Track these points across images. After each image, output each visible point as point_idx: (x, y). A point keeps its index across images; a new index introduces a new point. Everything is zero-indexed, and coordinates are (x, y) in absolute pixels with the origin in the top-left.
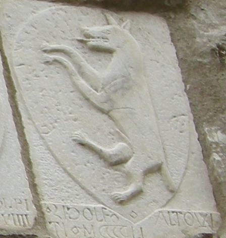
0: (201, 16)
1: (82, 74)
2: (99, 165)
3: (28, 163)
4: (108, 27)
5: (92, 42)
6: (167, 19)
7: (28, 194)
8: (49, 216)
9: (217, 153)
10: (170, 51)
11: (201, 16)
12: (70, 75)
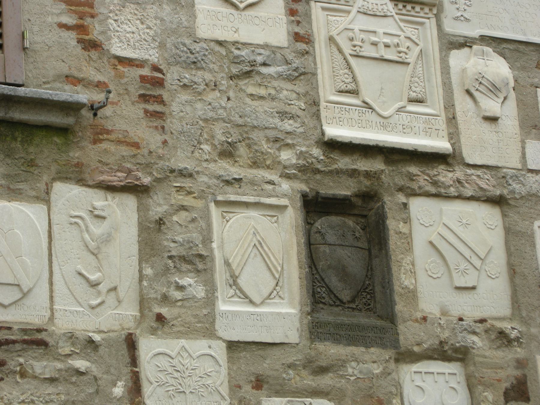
0: (155, 197)
1: (88, 231)
2: (85, 285)
3: (51, 283)
4: (106, 203)
5: (96, 212)
6: (138, 197)
7: (47, 304)
8: (57, 315)
9: (146, 281)
10: (134, 217)
11: (155, 197)
12: (82, 232)
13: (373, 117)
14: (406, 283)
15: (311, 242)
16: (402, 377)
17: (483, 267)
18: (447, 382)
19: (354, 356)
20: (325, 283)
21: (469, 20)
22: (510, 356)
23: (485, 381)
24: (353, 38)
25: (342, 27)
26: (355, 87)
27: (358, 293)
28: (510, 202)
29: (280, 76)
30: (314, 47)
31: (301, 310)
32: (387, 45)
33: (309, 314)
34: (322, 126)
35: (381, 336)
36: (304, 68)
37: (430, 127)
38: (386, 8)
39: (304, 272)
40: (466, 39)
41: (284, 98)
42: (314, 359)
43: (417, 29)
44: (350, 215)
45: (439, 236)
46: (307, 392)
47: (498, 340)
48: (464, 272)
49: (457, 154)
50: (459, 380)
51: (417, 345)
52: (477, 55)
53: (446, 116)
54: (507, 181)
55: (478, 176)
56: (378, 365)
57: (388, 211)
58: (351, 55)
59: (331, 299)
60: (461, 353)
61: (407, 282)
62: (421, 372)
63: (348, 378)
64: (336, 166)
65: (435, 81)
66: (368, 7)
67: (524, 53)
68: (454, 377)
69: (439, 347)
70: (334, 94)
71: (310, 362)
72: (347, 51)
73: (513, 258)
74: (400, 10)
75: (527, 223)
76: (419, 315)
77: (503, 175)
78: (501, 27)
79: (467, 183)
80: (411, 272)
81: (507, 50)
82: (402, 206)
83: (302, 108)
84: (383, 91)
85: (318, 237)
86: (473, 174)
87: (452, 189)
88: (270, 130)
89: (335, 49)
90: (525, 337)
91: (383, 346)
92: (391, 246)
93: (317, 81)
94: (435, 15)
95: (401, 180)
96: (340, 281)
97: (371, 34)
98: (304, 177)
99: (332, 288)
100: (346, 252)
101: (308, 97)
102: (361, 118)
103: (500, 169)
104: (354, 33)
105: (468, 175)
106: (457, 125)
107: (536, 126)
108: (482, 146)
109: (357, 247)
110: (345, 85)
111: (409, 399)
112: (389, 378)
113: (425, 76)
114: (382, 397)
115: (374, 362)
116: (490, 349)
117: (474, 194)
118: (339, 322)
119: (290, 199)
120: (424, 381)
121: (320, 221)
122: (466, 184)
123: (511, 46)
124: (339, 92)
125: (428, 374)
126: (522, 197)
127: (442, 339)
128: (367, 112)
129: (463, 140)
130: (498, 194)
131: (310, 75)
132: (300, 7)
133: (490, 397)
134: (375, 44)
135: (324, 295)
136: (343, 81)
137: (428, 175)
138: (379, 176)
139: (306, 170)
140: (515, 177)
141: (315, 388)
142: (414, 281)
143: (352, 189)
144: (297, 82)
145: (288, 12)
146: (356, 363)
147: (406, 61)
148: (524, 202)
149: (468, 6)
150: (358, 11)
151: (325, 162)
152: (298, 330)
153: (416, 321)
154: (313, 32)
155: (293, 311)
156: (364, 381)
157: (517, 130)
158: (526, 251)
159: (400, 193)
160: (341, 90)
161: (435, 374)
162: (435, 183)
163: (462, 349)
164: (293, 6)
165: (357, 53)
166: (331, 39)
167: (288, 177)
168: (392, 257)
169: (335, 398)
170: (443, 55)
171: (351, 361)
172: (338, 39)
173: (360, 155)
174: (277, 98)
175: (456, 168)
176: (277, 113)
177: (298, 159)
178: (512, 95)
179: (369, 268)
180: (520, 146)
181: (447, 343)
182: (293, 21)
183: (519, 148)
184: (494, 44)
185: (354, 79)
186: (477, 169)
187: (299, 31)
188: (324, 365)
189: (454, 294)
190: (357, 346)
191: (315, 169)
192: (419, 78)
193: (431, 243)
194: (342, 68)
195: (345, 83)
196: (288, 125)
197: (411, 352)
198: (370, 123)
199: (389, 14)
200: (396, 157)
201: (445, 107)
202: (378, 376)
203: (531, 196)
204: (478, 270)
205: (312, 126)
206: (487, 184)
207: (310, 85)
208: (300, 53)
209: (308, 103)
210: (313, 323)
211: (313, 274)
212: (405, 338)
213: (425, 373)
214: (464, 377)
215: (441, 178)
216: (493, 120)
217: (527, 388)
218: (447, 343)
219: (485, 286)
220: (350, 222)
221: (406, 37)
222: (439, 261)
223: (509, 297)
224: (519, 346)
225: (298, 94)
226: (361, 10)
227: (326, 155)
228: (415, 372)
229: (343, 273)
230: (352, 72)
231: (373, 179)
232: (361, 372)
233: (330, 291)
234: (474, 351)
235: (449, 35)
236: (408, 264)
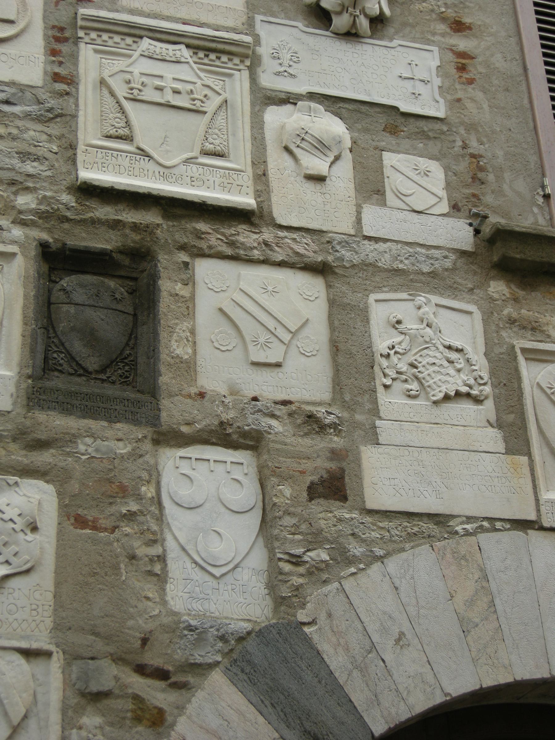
13: (151, 166)
14: (178, 352)
15: (51, 301)
16: (162, 462)
17: (294, 342)
18: (228, 472)
19: (90, 431)
20: (65, 348)
21: (294, 76)
22: (322, 445)
23: (281, 472)
24: (130, 81)
25: (117, 69)
26: (128, 132)
27: (112, 362)
28: (337, 270)
29: (27, 116)
30: (77, 89)
31: (19, 373)
32: (176, 90)
33: (29, 377)
34: (77, 170)
35: (133, 409)
36: (62, 109)
37: (230, 182)
38: (180, 54)
39: (29, 328)
40: (289, 95)
41: (29, 139)
42: (29, 430)
43: (224, 81)
44: (113, 276)
45: (232, 303)
46: (15, 470)
47: (306, 425)
48: (266, 345)
49: (265, 213)
50: (246, 471)
51: (186, 424)
52: (301, 111)
53: (253, 173)
54: (333, 247)
55: (294, 240)
56: (125, 444)
57: (162, 270)
58: (125, 98)
59: (72, 366)
60: (252, 438)
61: (182, 350)
62: (191, 458)
63: (77, 457)
64: (91, 215)
65: (241, 134)
66: (155, 51)
67: (367, 115)
68: (240, 467)
69: (218, 429)
70: (99, 139)
71: (24, 433)
72: (121, 91)
73: (336, 333)
74: (200, 58)
75: (359, 295)
76: (193, 390)
77: (328, 239)
78: (338, 87)
79: (277, 246)
80: (188, 341)
81: (344, 110)
82: (182, 265)
83: (54, 151)
84: (168, 139)
85: (62, 296)
86: (286, 237)
87: (256, 252)
88: (5, 171)
89: (105, 92)
90: (346, 424)
91: (136, 422)
92: (161, 309)
93: (77, 123)
94: (248, 67)
95: (184, 236)
96: (85, 346)
97: (156, 78)
98: (47, 225)
99: (74, 354)
100: (99, 314)
101: (64, 140)
102: (133, 165)
103: (325, 234)
104: (132, 76)
105: (279, 237)
106: (268, 182)
107: (379, 191)
108: (295, 203)
109: (116, 310)
110: (115, 129)
111: (168, 489)
112: (141, 460)
113: (230, 130)
114: (126, 482)
115: (119, 440)
116: (294, 435)
117: (286, 259)
118: (73, 389)
119: (21, 246)
120: (194, 469)
121: (67, 279)
122: (276, 248)
123: (351, 107)
124: (107, 137)
125: (201, 462)
126: (353, 266)
127: (223, 419)
128: (142, 160)
129: (274, 199)
130: (320, 260)
131: (68, 118)
132: (65, 48)
133: (288, 492)
134: (160, 89)
135: (61, 362)
136: (113, 126)
137: (223, 234)
138: (153, 230)
139: (48, 216)
140: (345, 244)
141: (27, 465)
142: (190, 351)
143: (113, 243)
144: (52, 125)
145: (49, 52)
146: (92, 440)
147: (201, 109)
148: (356, 271)
149: (295, 62)
150: (141, 55)
151: (76, 210)
152: (12, 395)
153: (189, 396)
154: (78, 74)
155: (8, 373)
156: (102, 461)
157: (352, 192)
158: (356, 327)
159: (183, 252)
160: (109, 134)
161: (212, 461)
162: (232, 244)
163: (254, 434)
164: (56, 46)
165: (134, 96)
166: (103, 82)
167: (24, 223)
168: (162, 322)
169: (55, 479)
170: (256, 110)
171: (85, 437)
172: (111, 82)
173: (128, 206)
174: (19, 138)
175: (264, 229)
176: (17, 153)
177: (40, 203)
178: (347, 157)
179: (132, 335)
180: (355, 210)
181: (232, 425)
182: (54, 61)
183: (352, 212)
184: (326, 103)
185: (128, 124)
186: (293, 231)
187: (60, 72)
188: (43, 437)
189: (250, 372)
190: (96, 420)
191: (62, 216)
192: (219, 130)
193: (221, 310)
194: (113, 111)
195: (115, 128)
196: (30, 167)
197: (177, 432)
198: (146, 172)
199: (183, 60)
200: (178, 211)
201: (253, 163)
202: (123, 457)
203: (366, 265)
204: (285, 344)
205: (64, 170)
206: (306, 249)
207: (68, 128)
208: (58, 94)
209: (63, 147)
210: (34, 388)
211: (50, 338)
212: (168, 416)
213: (196, 459)
214: (256, 468)
215: (241, 239)
216: (319, 179)
217: (344, 485)
218: (232, 425)
219: (294, 363)
220: (112, 283)
221: (203, 85)
222: (232, 331)
223: (330, 380)
224: (336, 435)
225: (50, 136)
226: (146, 54)
227: (79, 202)
228: (180, 457)
229: (91, 337)
230: (126, 117)
231: (144, 233)
232: (97, 450)
233: (72, 358)
234: (269, 436)
235: (266, 89)
236: (184, 331)
